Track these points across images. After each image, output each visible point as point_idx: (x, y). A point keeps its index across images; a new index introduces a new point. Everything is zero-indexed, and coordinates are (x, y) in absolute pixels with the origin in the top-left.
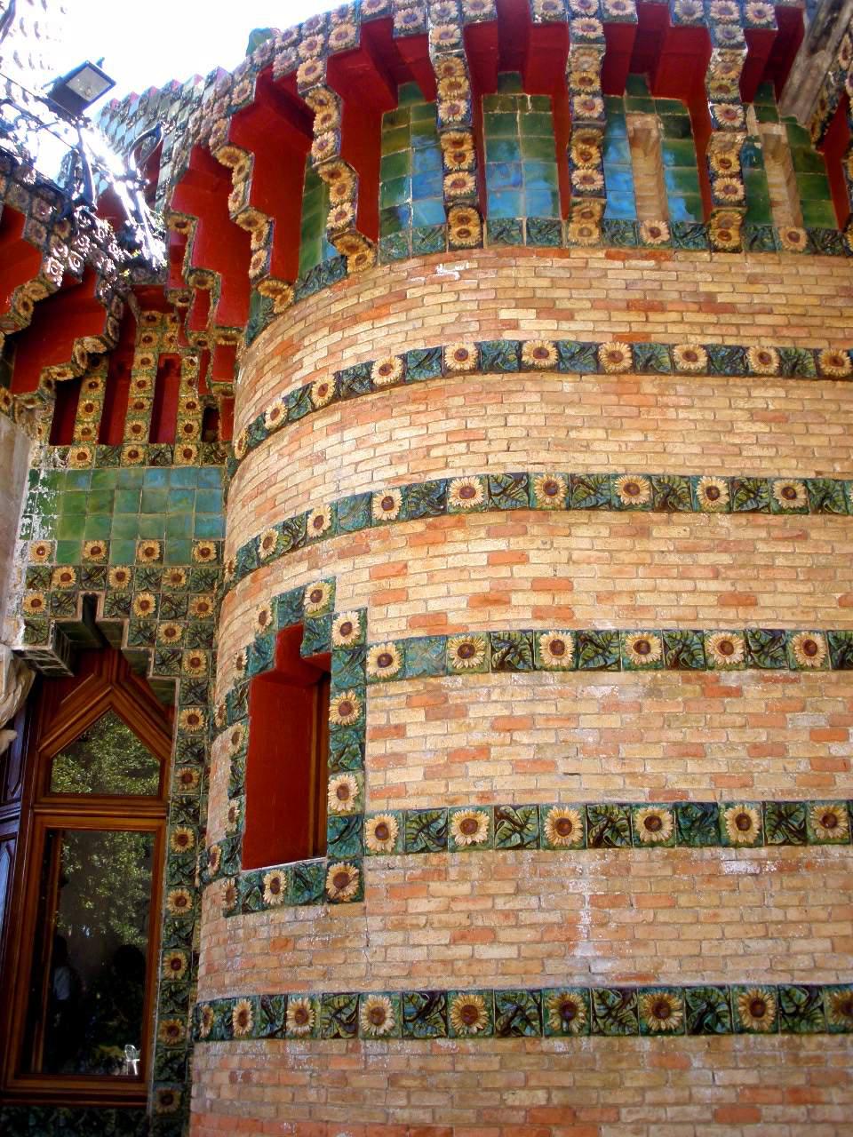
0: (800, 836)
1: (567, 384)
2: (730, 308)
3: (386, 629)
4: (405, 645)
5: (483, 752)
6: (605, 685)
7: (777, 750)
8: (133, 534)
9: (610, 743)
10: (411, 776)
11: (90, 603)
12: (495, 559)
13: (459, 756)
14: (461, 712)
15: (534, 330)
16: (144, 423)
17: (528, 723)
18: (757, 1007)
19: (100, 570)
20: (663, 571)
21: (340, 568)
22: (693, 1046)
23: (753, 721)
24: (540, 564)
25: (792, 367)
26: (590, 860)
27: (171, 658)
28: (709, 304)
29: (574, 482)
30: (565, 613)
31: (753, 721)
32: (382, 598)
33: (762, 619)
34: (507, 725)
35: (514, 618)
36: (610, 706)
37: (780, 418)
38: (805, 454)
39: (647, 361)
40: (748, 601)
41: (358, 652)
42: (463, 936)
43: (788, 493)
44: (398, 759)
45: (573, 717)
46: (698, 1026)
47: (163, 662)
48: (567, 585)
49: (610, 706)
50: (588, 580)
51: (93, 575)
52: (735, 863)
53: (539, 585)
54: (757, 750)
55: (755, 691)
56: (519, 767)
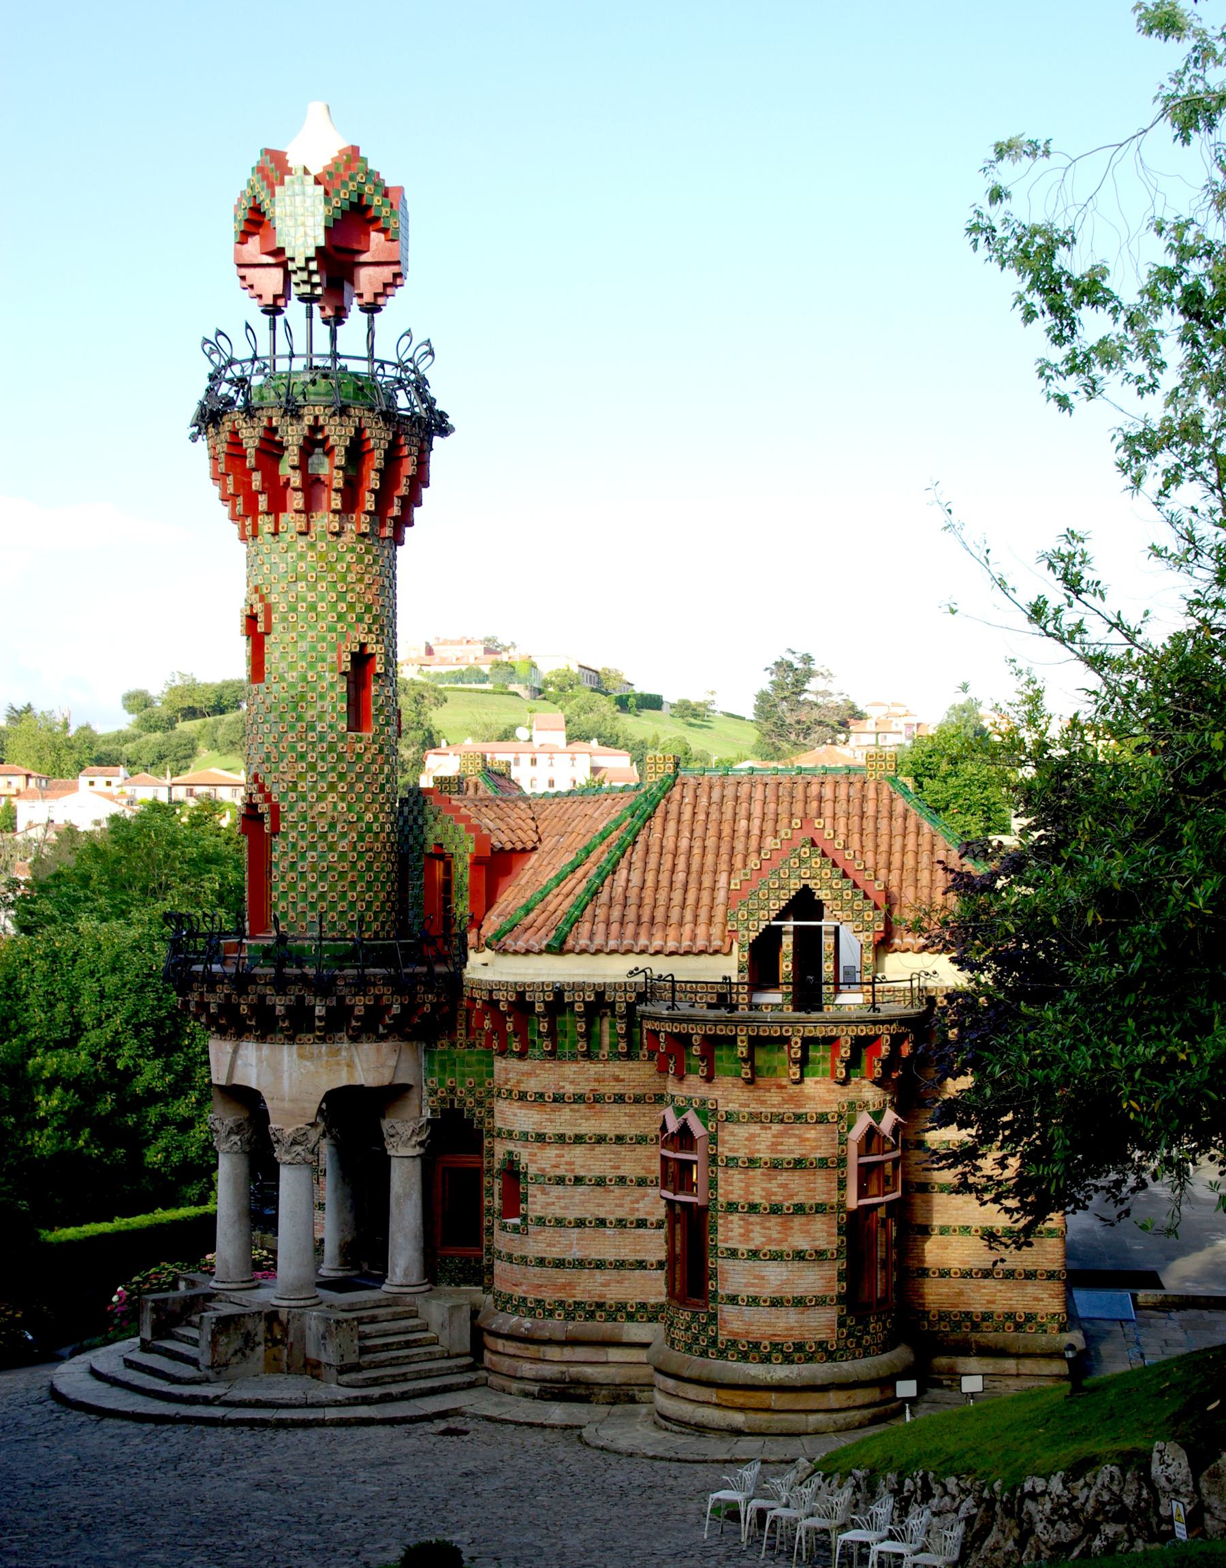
0: (625, 1226)
1: (576, 1106)
2: (623, 1080)
3: (532, 1170)
4: (536, 1175)
5: (553, 1204)
6: (581, 1189)
7: (622, 1206)
8: (464, 1075)
9: (582, 1202)
10: (538, 1207)
11: (452, 1101)
12: (558, 1156)
13: (548, 1204)
14: (548, 1194)
15: (569, 1089)
16: (463, 1032)
17: (563, 1197)
18: (611, 1264)
19: (454, 1088)
20: (597, 1159)
21: (521, 1150)
22: (597, 1271)
23: (617, 1198)
24: (566, 1158)
25: (638, 1100)
26: (576, 1230)
27: (481, 1122)
28: (617, 1079)
29: (576, 1136)
30: (572, 1170)
31: (617, 1198)
32: (531, 1161)
33: (621, 1173)
34: (559, 1198)
35: (560, 1172)
36: (583, 1194)
37: (633, 1115)
38: (638, 1126)
39: (598, 1099)
40: (618, 1168)
41: (526, 1173)
42: (549, 1245)
43: (631, 1139)
44: (535, 1203)
45: (573, 1197)
46: (598, 1267)
47: (480, 1123)
48: (572, 1163)
49: (583, 1194)
50: (579, 1162)
51: (452, 1090)
52: (609, 1232)
53: (567, 1163)
54: (617, 1205)
55: (618, 1191)
56: (561, 1208)
